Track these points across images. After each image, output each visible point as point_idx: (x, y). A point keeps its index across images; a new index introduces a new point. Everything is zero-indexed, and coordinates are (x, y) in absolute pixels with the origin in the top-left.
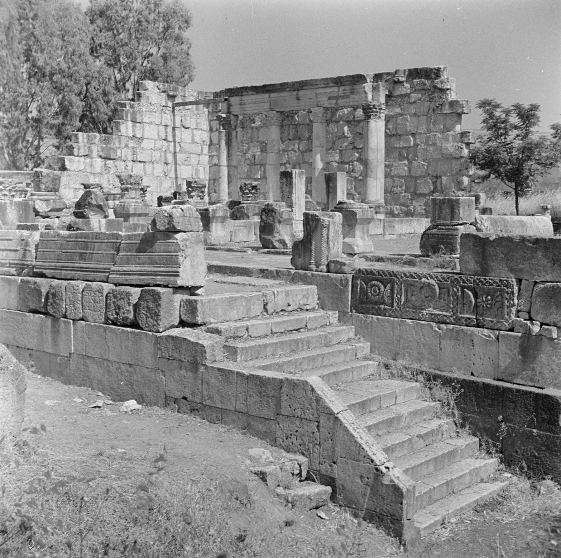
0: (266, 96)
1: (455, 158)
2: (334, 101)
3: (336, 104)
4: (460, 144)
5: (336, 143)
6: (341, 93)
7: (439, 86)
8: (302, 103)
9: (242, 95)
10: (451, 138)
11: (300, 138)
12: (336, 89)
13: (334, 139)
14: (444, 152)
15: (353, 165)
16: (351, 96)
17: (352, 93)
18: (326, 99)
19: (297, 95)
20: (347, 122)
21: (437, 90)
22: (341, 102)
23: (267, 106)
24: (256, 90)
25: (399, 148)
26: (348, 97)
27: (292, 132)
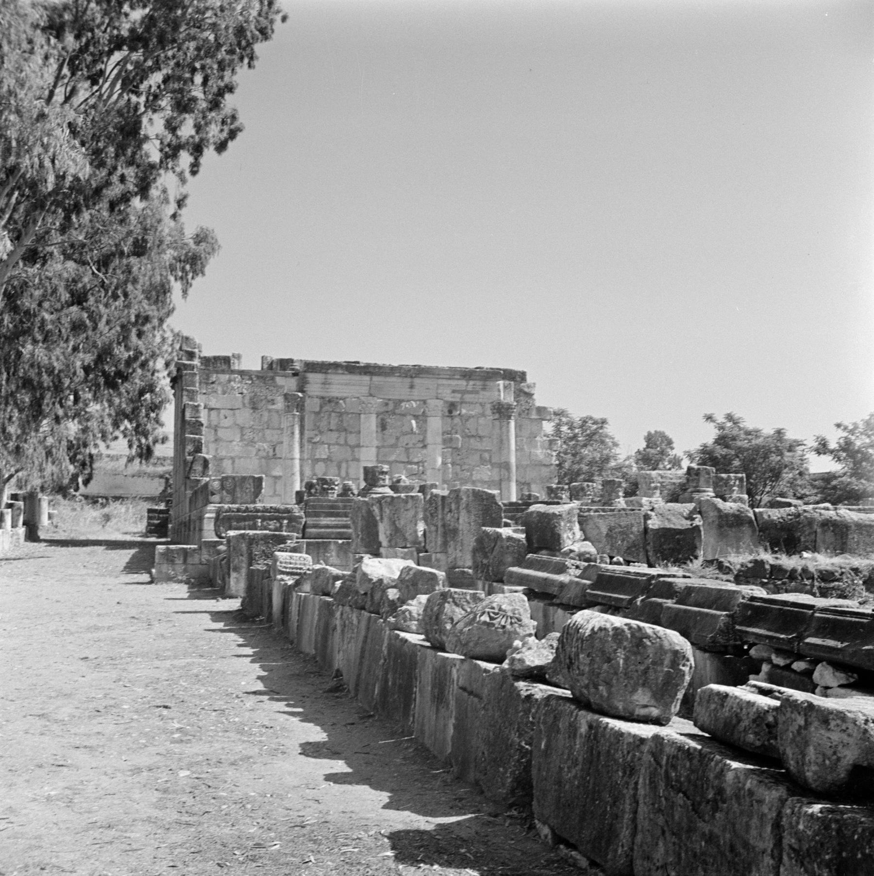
0: (366, 378)
1: (545, 465)
2: (459, 395)
3: (461, 398)
4: (549, 451)
5: (401, 439)
6: (470, 388)
7: (526, 390)
8: (416, 392)
9: (325, 373)
10: (539, 444)
11: (346, 430)
12: (464, 383)
13: (398, 434)
14: (534, 458)
15: (423, 466)
16: (482, 393)
17: (484, 389)
18: (449, 391)
19: (412, 382)
20: (414, 416)
21: (522, 394)
22: (468, 397)
23: (365, 390)
24: (352, 368)
25: (481, 450)
26: (477, 392)
27: (334, 421)
